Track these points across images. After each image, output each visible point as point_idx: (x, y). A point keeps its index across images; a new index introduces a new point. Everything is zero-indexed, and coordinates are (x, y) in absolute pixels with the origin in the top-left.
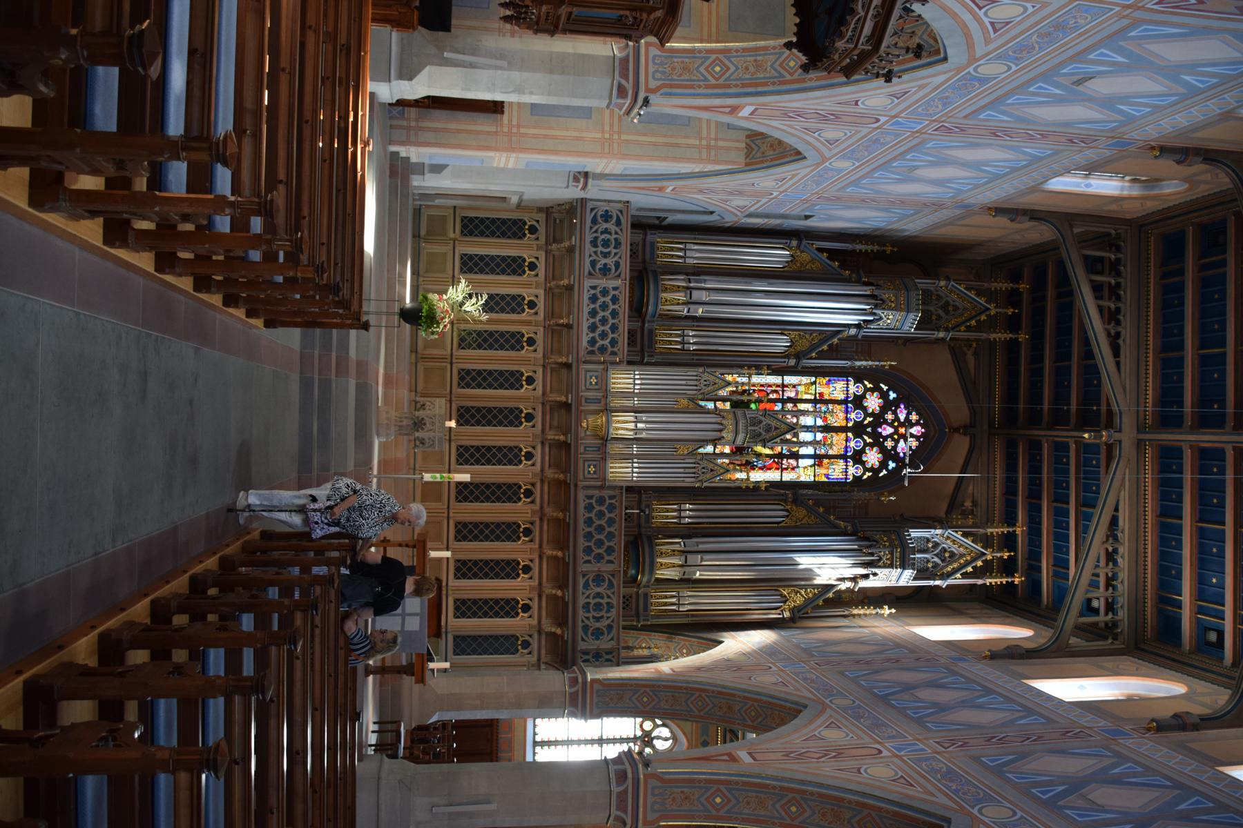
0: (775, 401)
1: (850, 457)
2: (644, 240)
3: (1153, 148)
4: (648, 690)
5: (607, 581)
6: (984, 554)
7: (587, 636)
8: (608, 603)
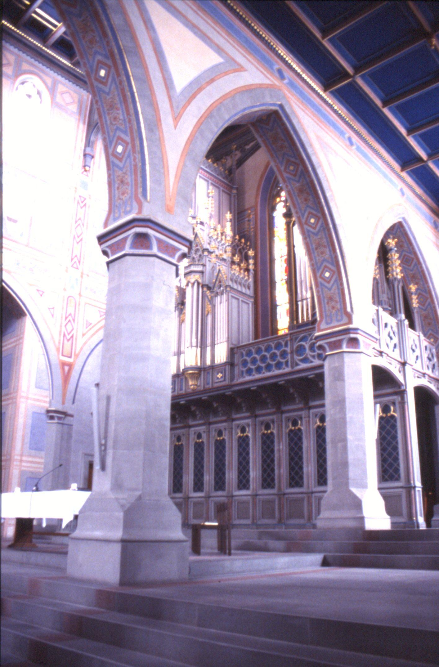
4: (318, 275)
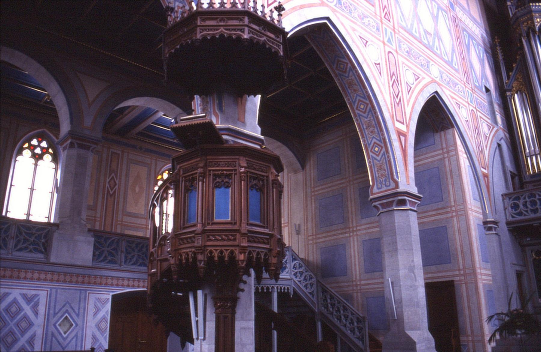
2: (530, 182)
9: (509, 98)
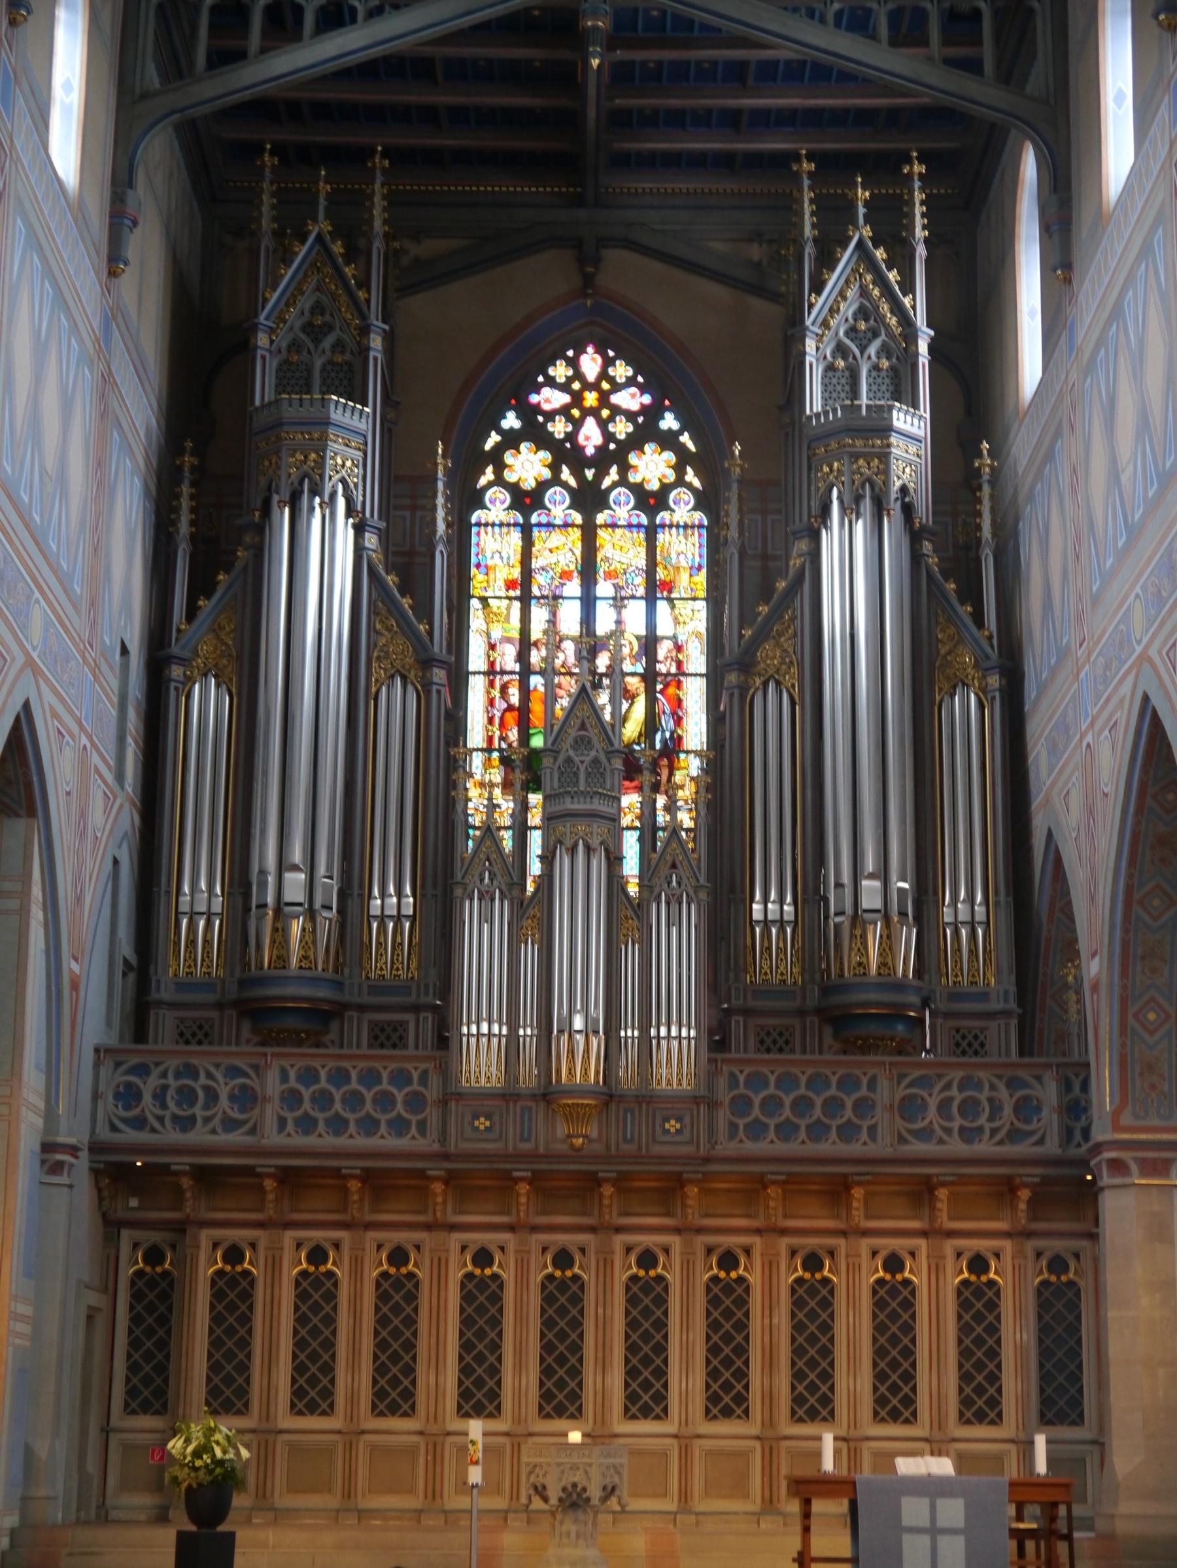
0: (525, 691)
1: (652, 518)
3: (13, 23)
4: (1132, 1010)
5: (913, 1090)
6: (861, 244)
7: (1031, 1133)
8: (961, 1088)
9: (176, 689)
